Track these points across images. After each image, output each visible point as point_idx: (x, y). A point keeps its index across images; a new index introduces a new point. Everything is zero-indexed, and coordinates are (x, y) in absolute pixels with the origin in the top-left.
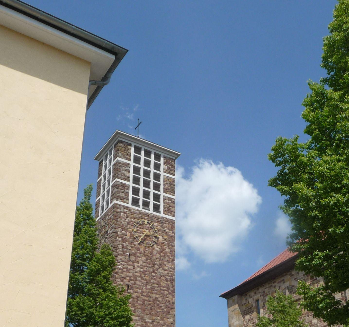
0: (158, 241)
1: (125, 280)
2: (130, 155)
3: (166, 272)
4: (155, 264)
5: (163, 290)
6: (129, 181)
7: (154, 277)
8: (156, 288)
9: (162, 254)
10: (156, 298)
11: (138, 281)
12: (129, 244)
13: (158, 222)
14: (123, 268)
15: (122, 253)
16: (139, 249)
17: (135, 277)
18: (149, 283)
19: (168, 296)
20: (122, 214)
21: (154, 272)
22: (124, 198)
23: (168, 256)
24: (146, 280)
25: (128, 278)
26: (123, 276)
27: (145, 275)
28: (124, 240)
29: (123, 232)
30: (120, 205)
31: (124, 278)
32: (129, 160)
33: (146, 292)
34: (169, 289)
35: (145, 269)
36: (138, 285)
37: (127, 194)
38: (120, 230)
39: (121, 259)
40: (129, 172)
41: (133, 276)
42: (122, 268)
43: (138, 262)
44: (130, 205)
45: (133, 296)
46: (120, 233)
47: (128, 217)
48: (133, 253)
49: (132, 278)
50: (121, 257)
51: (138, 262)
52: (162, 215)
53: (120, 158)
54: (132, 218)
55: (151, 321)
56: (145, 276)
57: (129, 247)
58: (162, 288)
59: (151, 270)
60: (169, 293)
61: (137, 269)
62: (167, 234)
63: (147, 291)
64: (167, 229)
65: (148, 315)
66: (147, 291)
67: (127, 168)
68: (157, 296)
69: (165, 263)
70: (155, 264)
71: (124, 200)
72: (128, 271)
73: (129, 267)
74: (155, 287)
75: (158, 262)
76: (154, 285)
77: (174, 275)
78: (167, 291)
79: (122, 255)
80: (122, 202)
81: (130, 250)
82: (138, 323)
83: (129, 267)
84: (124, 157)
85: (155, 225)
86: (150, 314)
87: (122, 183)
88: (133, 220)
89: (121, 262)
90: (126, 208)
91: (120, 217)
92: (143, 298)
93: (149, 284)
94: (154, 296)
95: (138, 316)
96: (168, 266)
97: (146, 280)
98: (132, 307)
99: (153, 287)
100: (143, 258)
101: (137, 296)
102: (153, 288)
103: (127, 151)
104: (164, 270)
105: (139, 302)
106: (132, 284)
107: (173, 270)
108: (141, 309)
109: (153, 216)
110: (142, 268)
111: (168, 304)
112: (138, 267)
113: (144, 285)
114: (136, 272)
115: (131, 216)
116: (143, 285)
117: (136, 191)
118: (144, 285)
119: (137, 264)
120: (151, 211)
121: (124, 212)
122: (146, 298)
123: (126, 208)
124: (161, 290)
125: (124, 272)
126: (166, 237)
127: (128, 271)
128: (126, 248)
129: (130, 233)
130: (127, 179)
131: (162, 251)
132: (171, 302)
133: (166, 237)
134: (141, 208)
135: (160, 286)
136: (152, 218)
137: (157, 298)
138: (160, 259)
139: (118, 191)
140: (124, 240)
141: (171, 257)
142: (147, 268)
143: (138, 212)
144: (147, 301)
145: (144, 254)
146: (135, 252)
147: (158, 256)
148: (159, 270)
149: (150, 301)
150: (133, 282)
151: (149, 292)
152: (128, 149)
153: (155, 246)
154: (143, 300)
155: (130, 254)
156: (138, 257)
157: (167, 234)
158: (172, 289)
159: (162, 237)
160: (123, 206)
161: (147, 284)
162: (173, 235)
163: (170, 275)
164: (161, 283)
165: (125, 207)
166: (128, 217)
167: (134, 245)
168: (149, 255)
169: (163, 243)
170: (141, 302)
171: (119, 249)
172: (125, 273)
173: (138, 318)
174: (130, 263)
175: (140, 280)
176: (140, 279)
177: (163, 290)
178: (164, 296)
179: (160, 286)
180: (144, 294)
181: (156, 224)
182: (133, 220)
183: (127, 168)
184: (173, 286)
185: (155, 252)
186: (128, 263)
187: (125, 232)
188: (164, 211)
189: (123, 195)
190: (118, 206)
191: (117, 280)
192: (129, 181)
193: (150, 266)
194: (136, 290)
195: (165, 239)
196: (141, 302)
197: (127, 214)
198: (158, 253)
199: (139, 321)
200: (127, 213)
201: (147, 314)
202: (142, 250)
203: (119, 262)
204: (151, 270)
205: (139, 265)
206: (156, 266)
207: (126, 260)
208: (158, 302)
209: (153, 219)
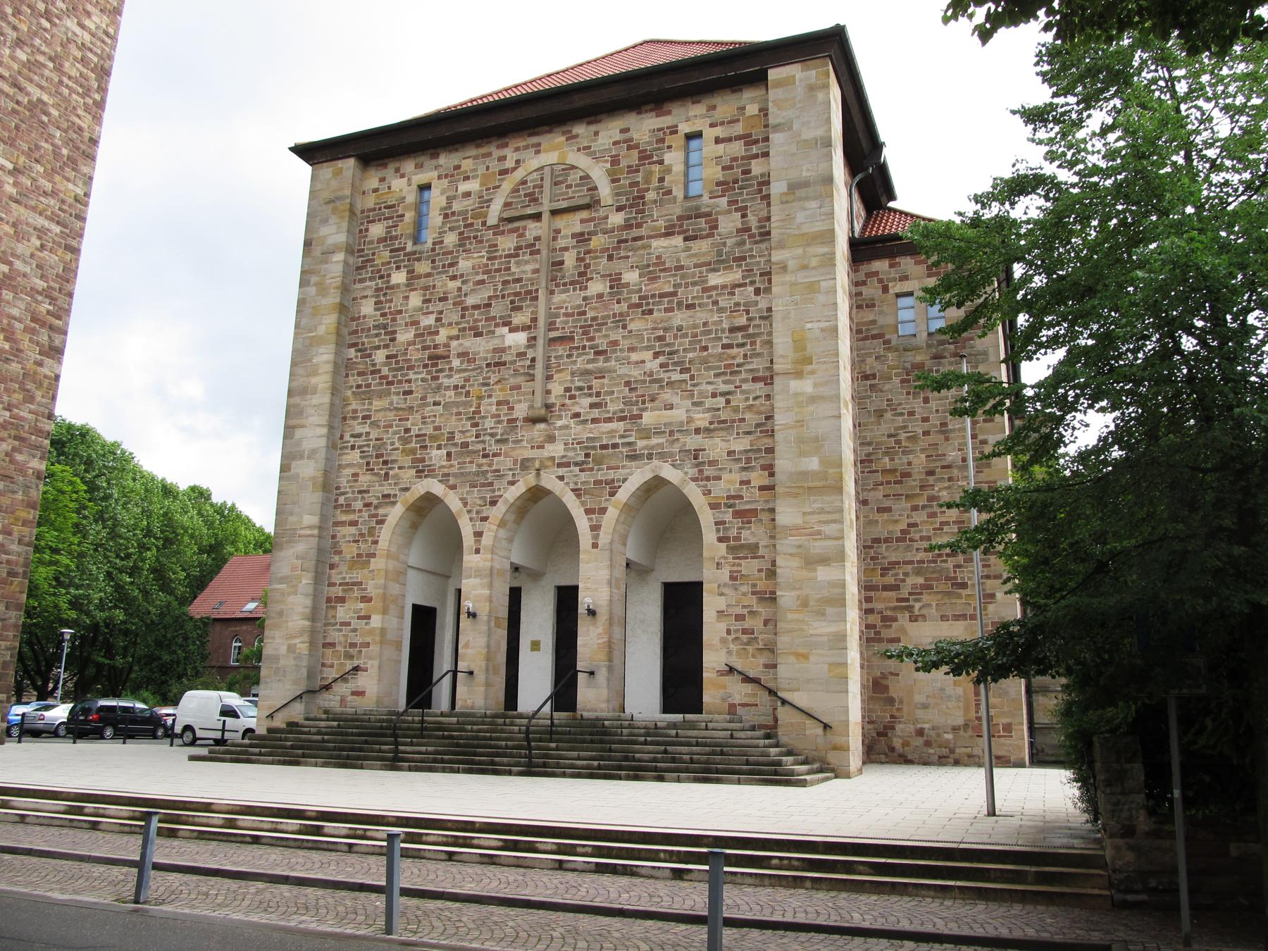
137: (45, 104)
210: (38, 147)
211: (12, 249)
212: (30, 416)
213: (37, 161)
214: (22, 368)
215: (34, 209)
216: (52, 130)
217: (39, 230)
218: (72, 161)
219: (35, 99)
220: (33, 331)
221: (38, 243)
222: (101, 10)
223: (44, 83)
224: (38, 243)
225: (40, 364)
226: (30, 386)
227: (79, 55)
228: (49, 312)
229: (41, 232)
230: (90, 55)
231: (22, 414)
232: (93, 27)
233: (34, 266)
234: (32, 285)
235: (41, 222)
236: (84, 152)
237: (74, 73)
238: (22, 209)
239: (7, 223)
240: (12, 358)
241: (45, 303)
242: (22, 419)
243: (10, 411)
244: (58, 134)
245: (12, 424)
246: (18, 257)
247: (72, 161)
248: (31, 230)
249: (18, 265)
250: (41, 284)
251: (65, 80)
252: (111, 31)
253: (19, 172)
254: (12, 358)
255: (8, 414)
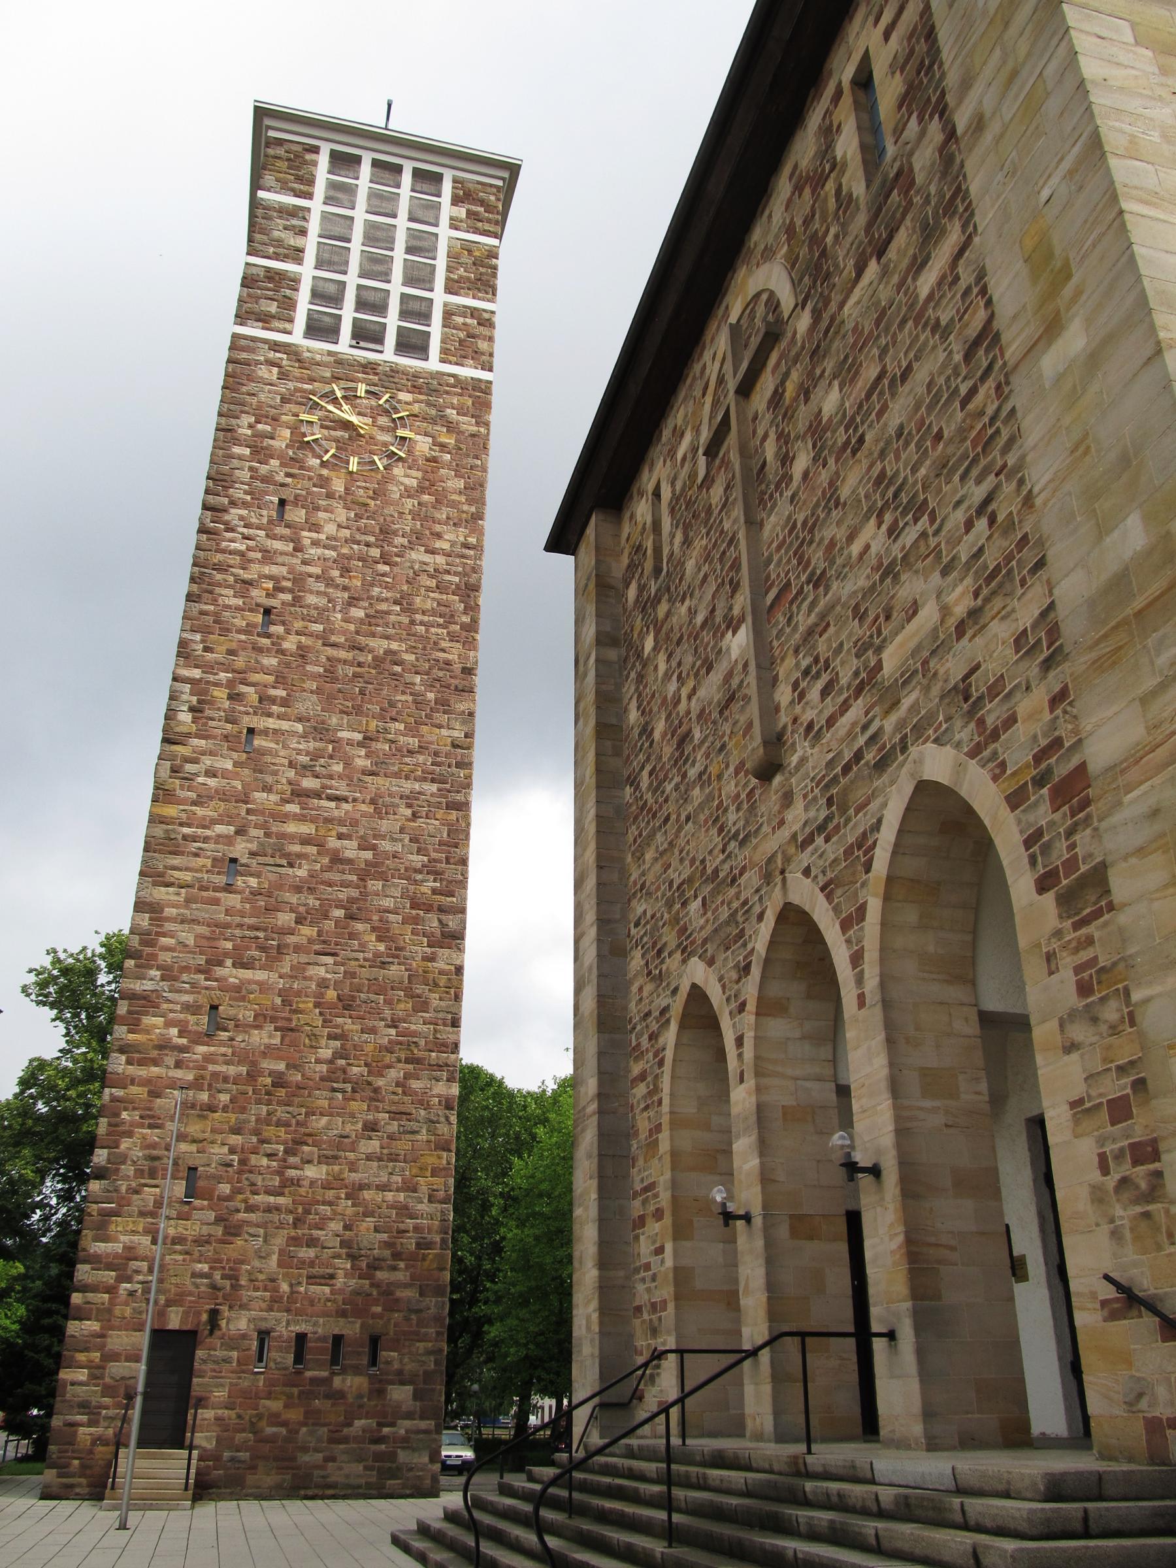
0: (410, 452)
1: (255, 593)
2: (311, 182)
3: (440, 560)
4: (395, 533)
5: (422, 623)
6: (299, 261)
7: (388, 580)
8: (392, 618)
9: (426, 497)
10: (389, 652)
11: (311, 592)
12: (282, 465)
13: (416, 389)
14: (249, 549)
15: (248, 498)
16: (324, 482)
17: (299, 580)
18: (363, 600)
19: (444, 644)
20: (263, 372)
21: (385, 559)
22: (274, 317)
23: (453, 504)
24: (345, 588)
25: (270, 585)
26: (246, 576)
27: (345, 571)
28: (260, 453)
29: (260, 426)
30: (254, 339)
31: (251, 584)
32: (309, 196)
33: (344, 632)
34: (450, 619)
35: (345, 551)
36: (309, 606)
37: (289, 305)
38: (249, 419)
39: (241, 518)
40: (303, 232)
41: (291, 576)
42: (243, 547)
43: (315, 527)
44: (297, 336)
45: (286, 645)
46: (249, 432)
47: (283, 376)
48: (296, 497)
49: (289, 584)
50: (244, 512)
51: (315, 527)
52: (434, 363)
53: (269, 190)
54: (301, 380)
55: (359, 737)
56: (342, 576)
57: (280, 477)
58: (418, 617)
59: (375, 552)
60: (448, 633)
61: (312, 551)
62: (451, 427)
63: (352, 627)
64: (454, 412)
65: (347, 714)
66: (352, 627)
67: (294, 222)
68: (394, 646)
69: (438, 528)
70: (395, 533)
71: (276, 324)
72: (268, 556)
73: (278, 545)
74: (388, 613)
75: (408, 525)
76: (384, 607)
77: (476, 570)
78: (439, 626)
79: (245, 505)
80: (263, 328)
81: (283, 485)
82: (301, 747)
83: (278, 545)
84: (285, 188)
85: (399, 402)
86: (358, 710)
87: (268, 270)
88: (306, 386)
89: (245, 531)
90: (277, 348)
91: (250, 378)
92: (330, 651)
93: (362, 604)
94: (380, 645)
95: (300, 720)
96: (451, 537)
97: (345, 588)
98: (274, 687)
99: (377, 612)
100: (342, 514)
101: (300, 647)
102: (372, 618)
103: (298, 168)
104: (432, 552)
105: (309, 668)
106: (283, 603)
107: (472, 552)
108: (318, 691)
109: (395, 371)
110: (334, 548)
111: (441, 674)
112: (315, 543)
113: (338, 608)
114: (304, 563)
115: (297, 372)
116: (334, 607)
117: (328, 295)
118: (338, 608)
119: (314, 535)
120: (388, 354)
121: (272, 363)
122: (342, 654)
123: (277, 348)
124: (412, 622)
125: (250, 561)
126: (450, 441)
127: (268, 556)
128: (266, 479)
129: (289, 431)
130: (297, 255)
131: (428, 484)
132: (457, 667)
133: (450, 441)
134: (344, 345)
135: (409, 610)
136: (391, 377)
137: (394, 653)
138: (415, 515)
139: (249, 295)
140: (260, 453)
141: (465, 508)
142: (355, 547)
143: (332, 359)
144: (345, 662)
145: (348, 499)
146: (304, 493)
147: (409, 504)
148: (414, 555)
149: (360, 665)
150: (288, 597)
151: (357, 633)
152: (306, 162)
153: (398, 471)
154: (328, 659)
155: (282, 503)
156: (317, 509)
157: (451, 427)
158: (466, 619)
159: (430, 440)
160: (265, 341)
161: (353, 601)
162: (482, 430)
163: (460, 569)
164: (418, 600)
165: (275, 346)
166: (283, 376)
167: (301, 468)
168: (372, 503)
169: (434, 460)
170: (321, 670)
171: (237, 485)
172: (255, 567)
173: (299, 727)
174: (280, 530)
175: (322, 589)
176: (321, 587)
177: (422, 623)
178: (427, 645)
179: (409, 610)
180: (334, 639)
181: (404, 396)
182: (306, 386)
183: (294, 222)
184: (472, 608)
185: (395, 492)
186: (272, 530)
187: (269, 428)
188: (444, 351)
189: (273, 308)
190: (243, 342)
191: (218, 590)
192: (299, 261)
193: (372, 539)
194: (298, 625)
195: (443, 446)
196: (321, 670)
197: (280, 367)
198: (408, 493)
199: (305, 736)
200: (285, 363)
201: (342, 712)
202: (338, 486)
203: (232, 530)
204: (375, 552)
205: (323, 537)
206: (399, 540)
207: (265, 521)
208: (398, 669)
209: (396, 380)
210: (392, 704)
211: (373, 829)
212: (425, 1028)
213: (394, 719)
214: (406, 970)
215: (397, 775)
216: (408, 677)
217: (408, 797)
218: (443, 704)
219: (381, 652)
220: (416, 920)
221: (409, 812)
222: (455, 524)
223: (391, 631)
224: (409, 812)
225: (432, 959)
226: (420, 989)
227: (433, 583)
228: (434, 891)
229: (410, 799)
230: (448, 577)
231: (413, 1027)
232: (446, 546)
233: (407, 841)
234: (407, 864)
235: (408, 786)
236: (456, 689)
237: (429, 605)
238: (380, 780)
239: (363, 802)
240: (390, 960)
241: (427, 881)
242: (414, 1034)
243: (396, 1027)
244: (418, 679)
245: (401, 1043)
246: (383, 838)
247: (443, 704)
248: (397, 800)
249: (386, 846)
250: (418, 860)
251: (418, 617)
252: (472, 540)
253: (371, 740)
254: (390, 960)
255: (393, 1031)
